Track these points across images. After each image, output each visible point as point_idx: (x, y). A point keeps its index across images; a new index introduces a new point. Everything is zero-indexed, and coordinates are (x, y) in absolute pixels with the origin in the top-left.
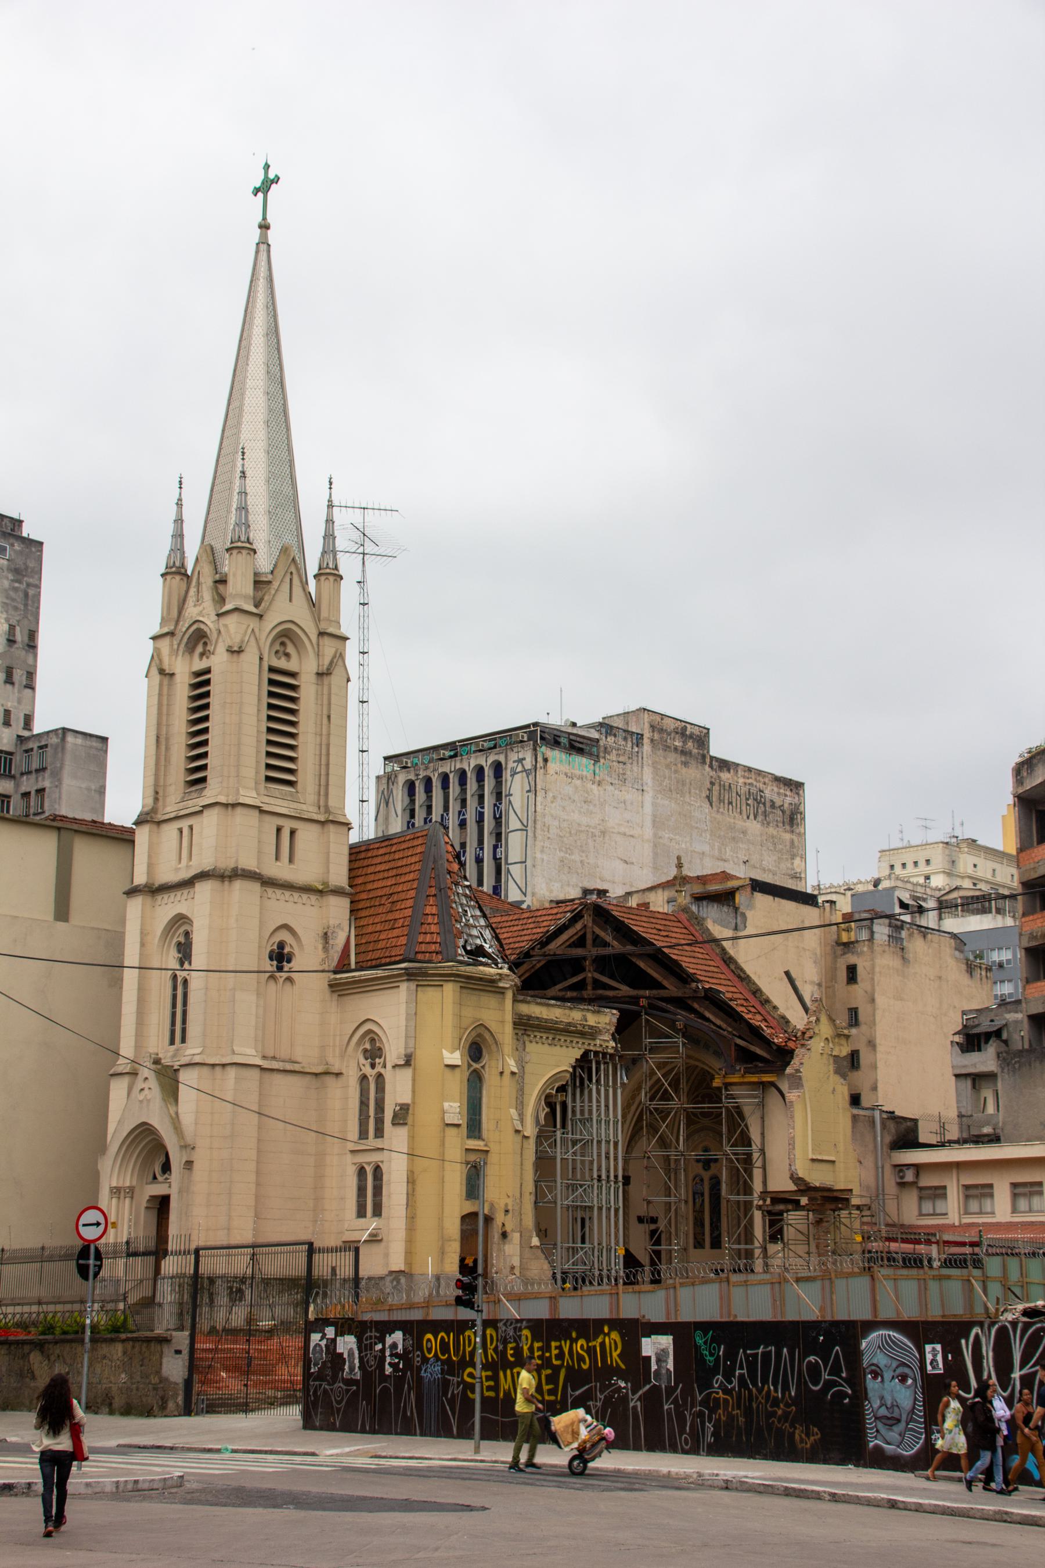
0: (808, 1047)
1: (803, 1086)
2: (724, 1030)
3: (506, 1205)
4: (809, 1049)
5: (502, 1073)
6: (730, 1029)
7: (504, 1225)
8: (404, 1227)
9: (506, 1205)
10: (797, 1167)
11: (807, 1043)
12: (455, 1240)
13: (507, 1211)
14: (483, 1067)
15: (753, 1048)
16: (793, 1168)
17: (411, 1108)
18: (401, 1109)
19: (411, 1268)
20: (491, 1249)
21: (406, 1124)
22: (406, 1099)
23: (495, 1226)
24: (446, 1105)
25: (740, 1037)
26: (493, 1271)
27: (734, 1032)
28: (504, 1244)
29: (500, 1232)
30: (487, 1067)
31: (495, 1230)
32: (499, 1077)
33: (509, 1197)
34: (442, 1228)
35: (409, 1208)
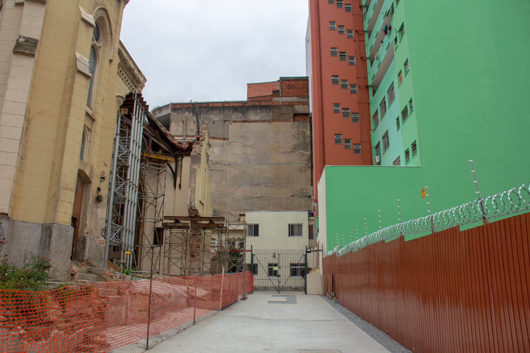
0: (201, 145)
1: (200, 162)
2: (147, 132)
3: (103, 172)
4: (202, 146)
5: (111, 61)
6: (150, 132)
7: (99, 189)
8: (15, 164)
9: (103, 172)
10: (195, 204)
11: (200, 142)
12: (71, 190)
13: (103, 178)
14: (99, 47)
15: (160, 144)
16: (193, 204)
17: (39, 43)
18: (26, 41)
19: (12, 213)
20: (85, 210)
21: (33, 56)
22: (35, 35)
23: (91, 190)
24: (78, 55)
25: (154, 137)
26: (86, 231)
27: (152, 134)
28: (97, 207)
29: (96, 196)
30: (102, 49)
31: (91, 193)
32: (108, 63)
33: (106, 165)
34: (59, 174)
35: (21, 145)
